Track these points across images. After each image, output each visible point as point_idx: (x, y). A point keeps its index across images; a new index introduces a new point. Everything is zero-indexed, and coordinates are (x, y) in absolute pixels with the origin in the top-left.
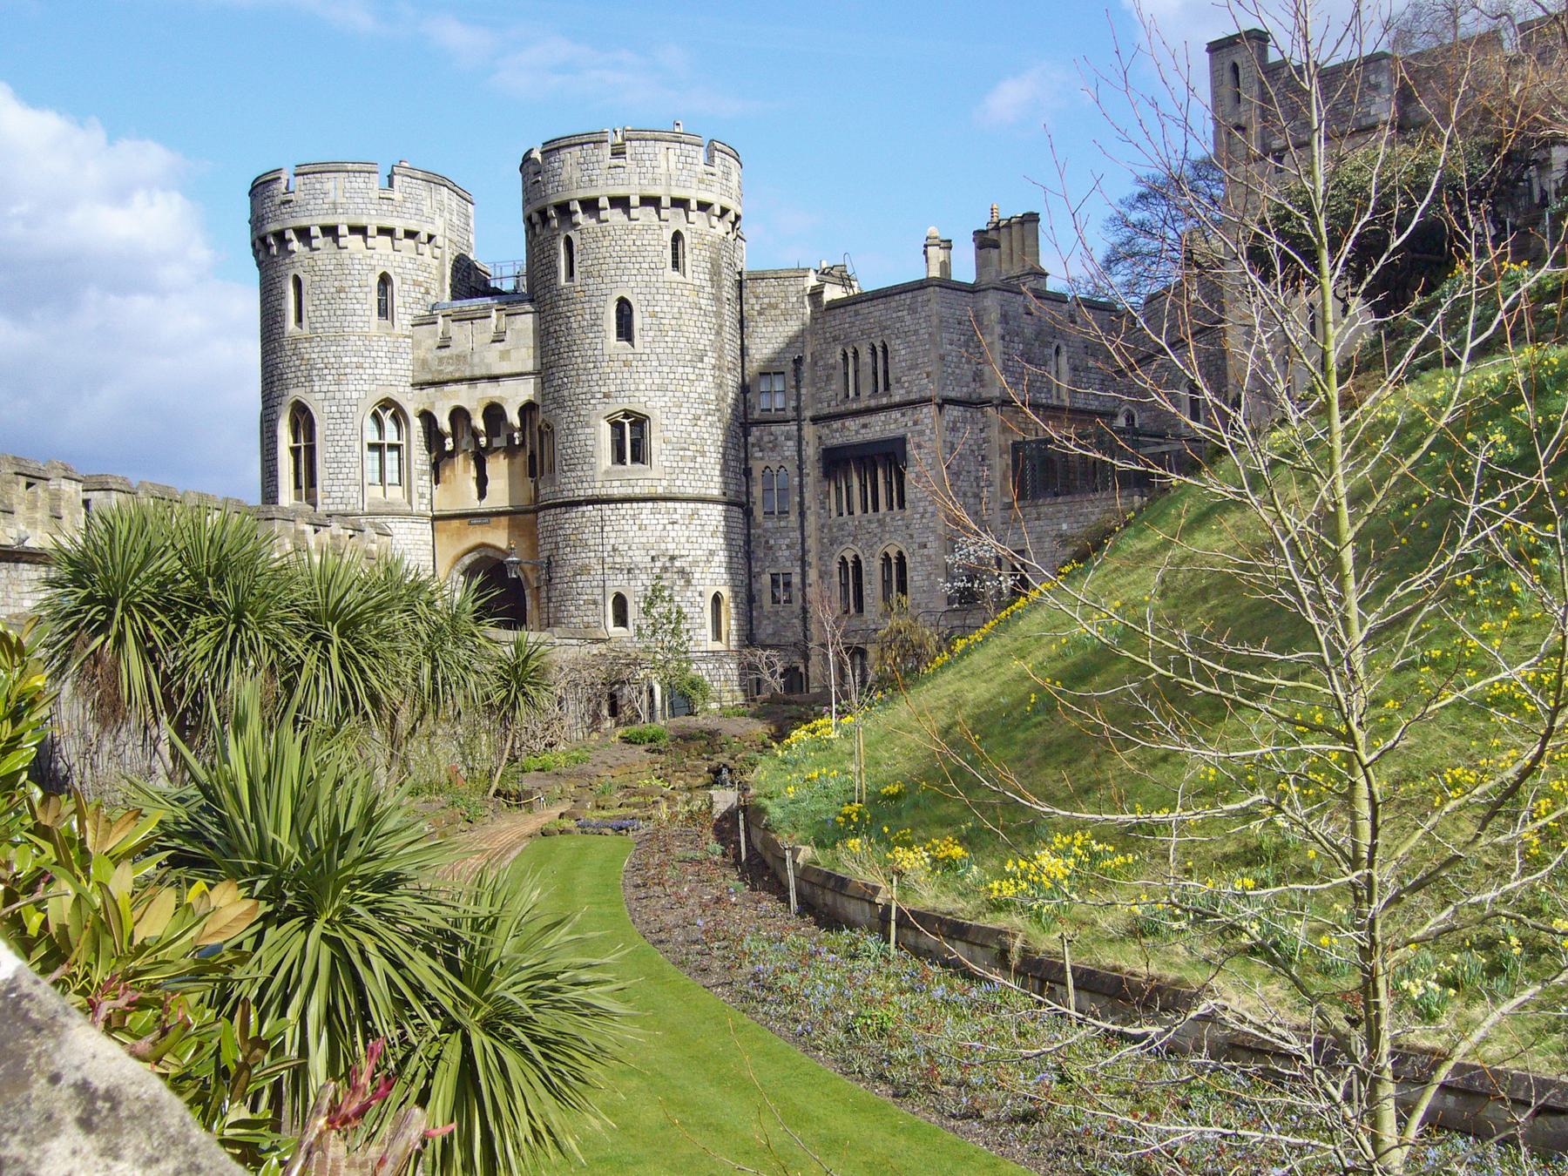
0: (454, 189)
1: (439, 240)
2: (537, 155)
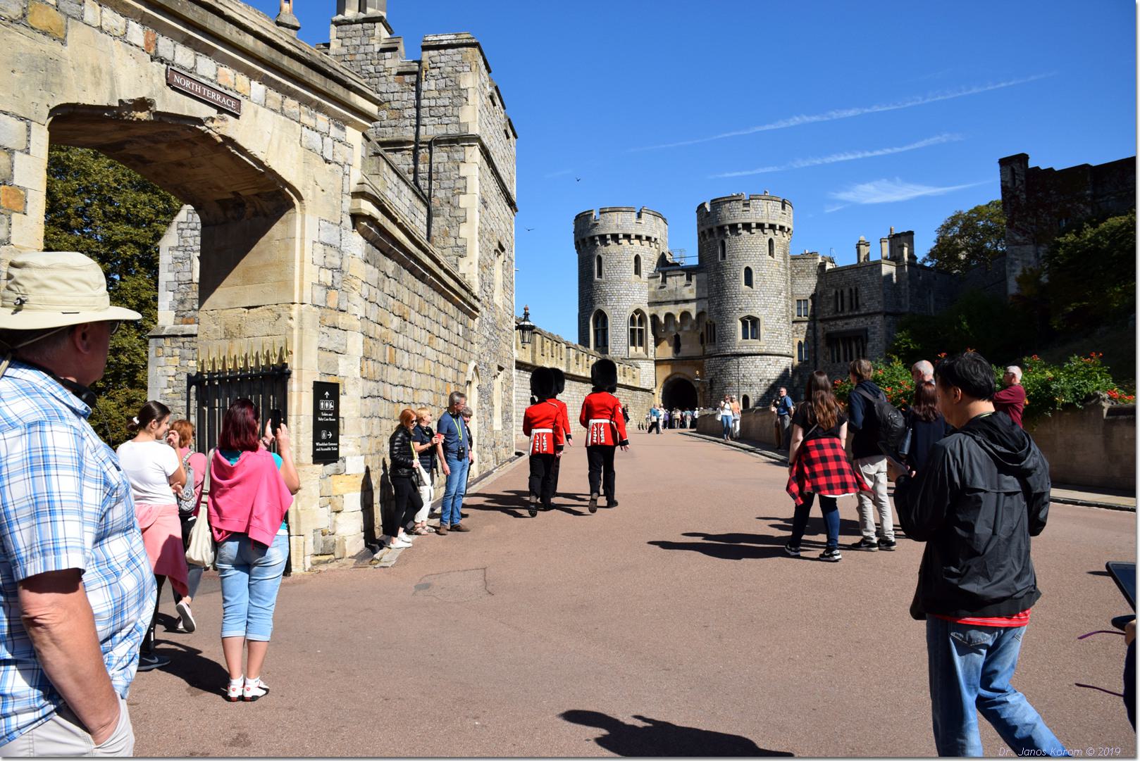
0: (664, 220)
1: (658, 240)
2: (708, 207)
